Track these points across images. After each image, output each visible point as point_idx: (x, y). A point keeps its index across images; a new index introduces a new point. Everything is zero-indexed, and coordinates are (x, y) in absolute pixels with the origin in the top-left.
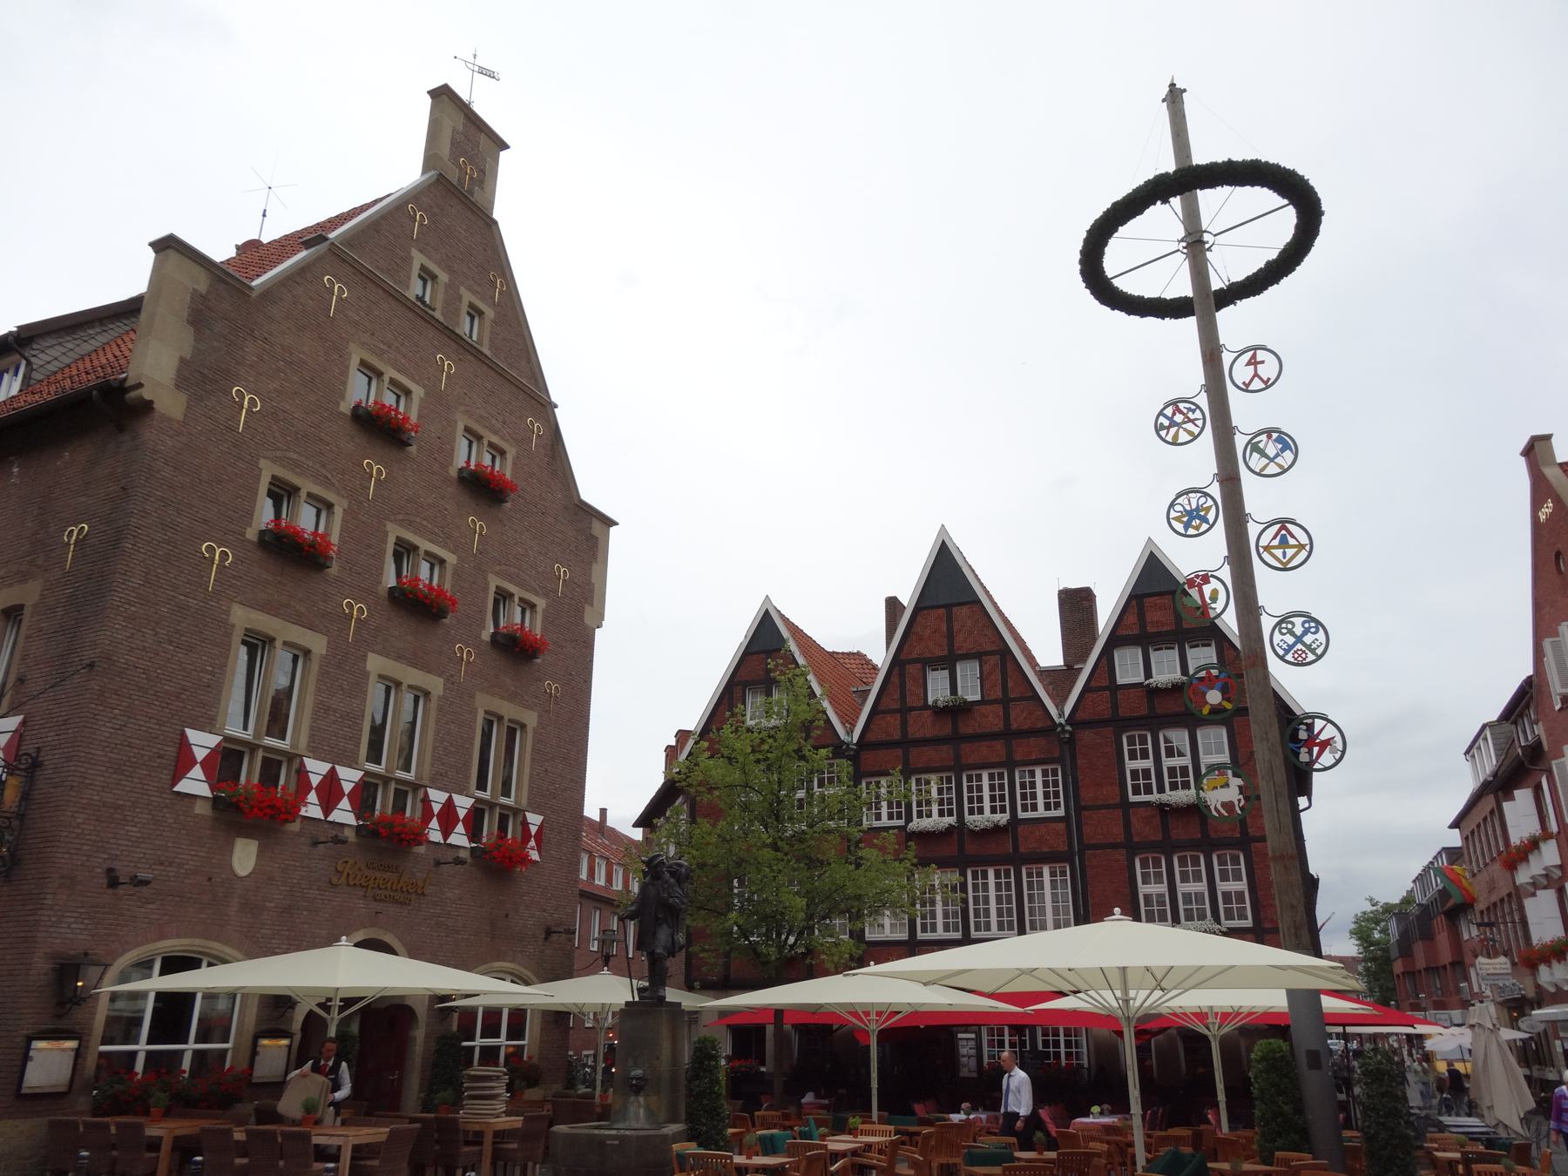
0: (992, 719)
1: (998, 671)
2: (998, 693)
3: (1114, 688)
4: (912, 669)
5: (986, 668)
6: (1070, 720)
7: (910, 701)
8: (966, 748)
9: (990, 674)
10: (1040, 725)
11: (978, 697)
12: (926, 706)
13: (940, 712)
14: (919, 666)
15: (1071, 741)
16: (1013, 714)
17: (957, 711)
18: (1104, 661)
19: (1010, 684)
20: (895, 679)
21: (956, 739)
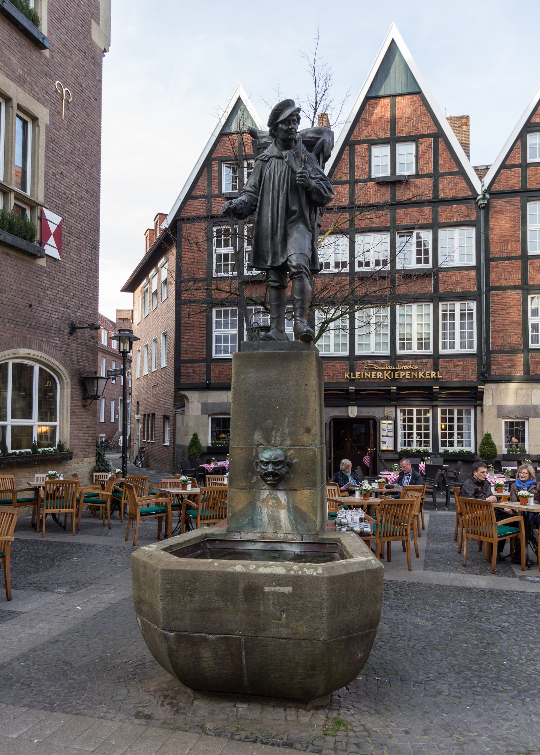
0: (424, 189)
1: (431, 151)
2: (430, 169)
3: (525, 166)
4: (360, 149)
5: (422, 148)
6: (488, 190)
7: (357, 174)
8: (400, 212)
9: (424, 153)
10: (462, 195)
11: (413, 172)
12: (370, 179)
13: (382, 183)
14: (365, 146)
15: (487, 208)
16: (441, 186)
17: (393, 183)
18: (519, 143)
19: (440, 162)
20: (346, 157)
21: (394, 205)
